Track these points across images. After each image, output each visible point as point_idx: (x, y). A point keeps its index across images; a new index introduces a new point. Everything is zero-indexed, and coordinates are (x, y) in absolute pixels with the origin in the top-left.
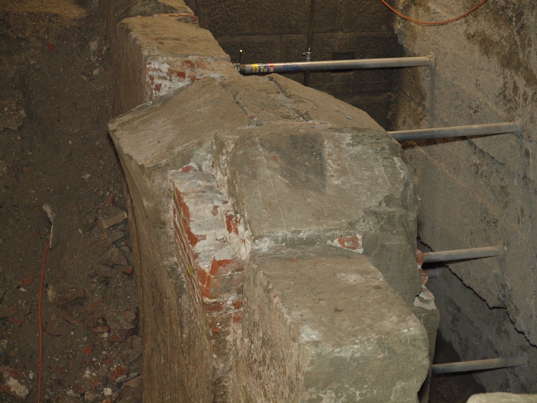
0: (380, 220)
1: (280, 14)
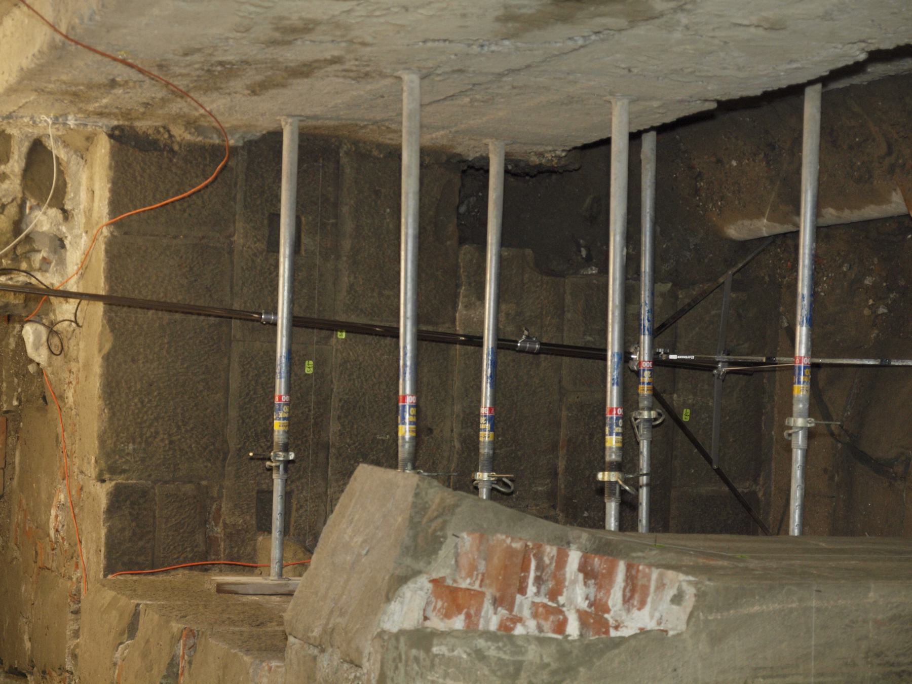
1: (198, 341)
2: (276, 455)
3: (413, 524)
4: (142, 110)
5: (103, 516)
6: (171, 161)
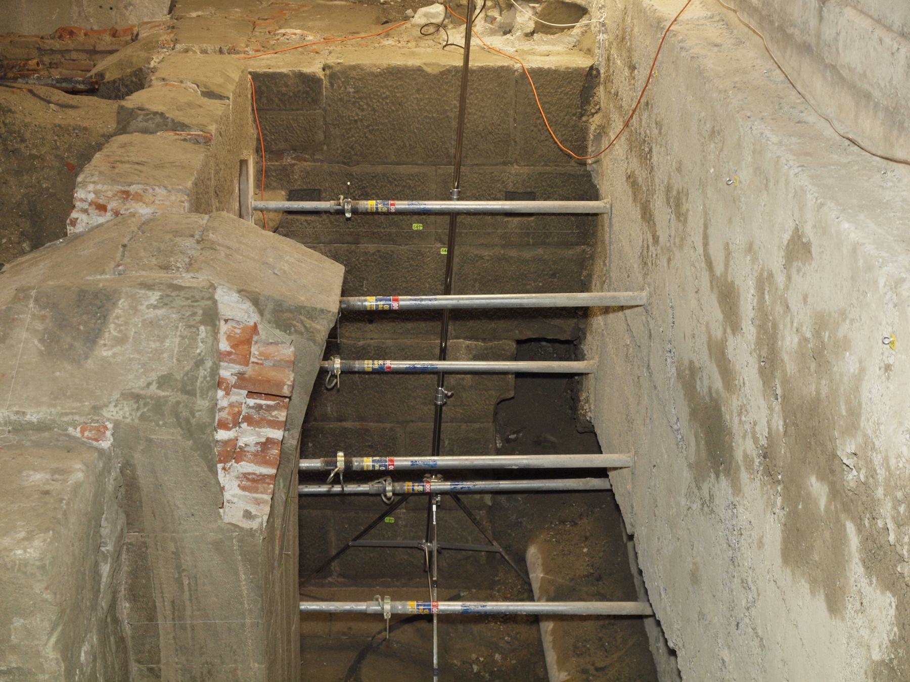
0: (142, 406)
2: (348, 203)
3: (299, 309)
4: (613, 91)
5: (296, 69)
6: (574, 115)
